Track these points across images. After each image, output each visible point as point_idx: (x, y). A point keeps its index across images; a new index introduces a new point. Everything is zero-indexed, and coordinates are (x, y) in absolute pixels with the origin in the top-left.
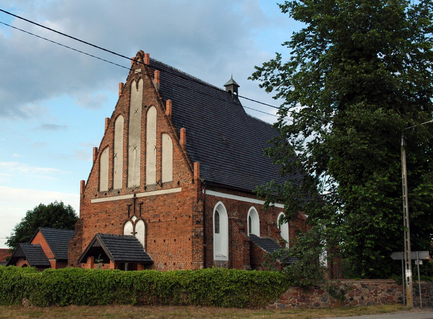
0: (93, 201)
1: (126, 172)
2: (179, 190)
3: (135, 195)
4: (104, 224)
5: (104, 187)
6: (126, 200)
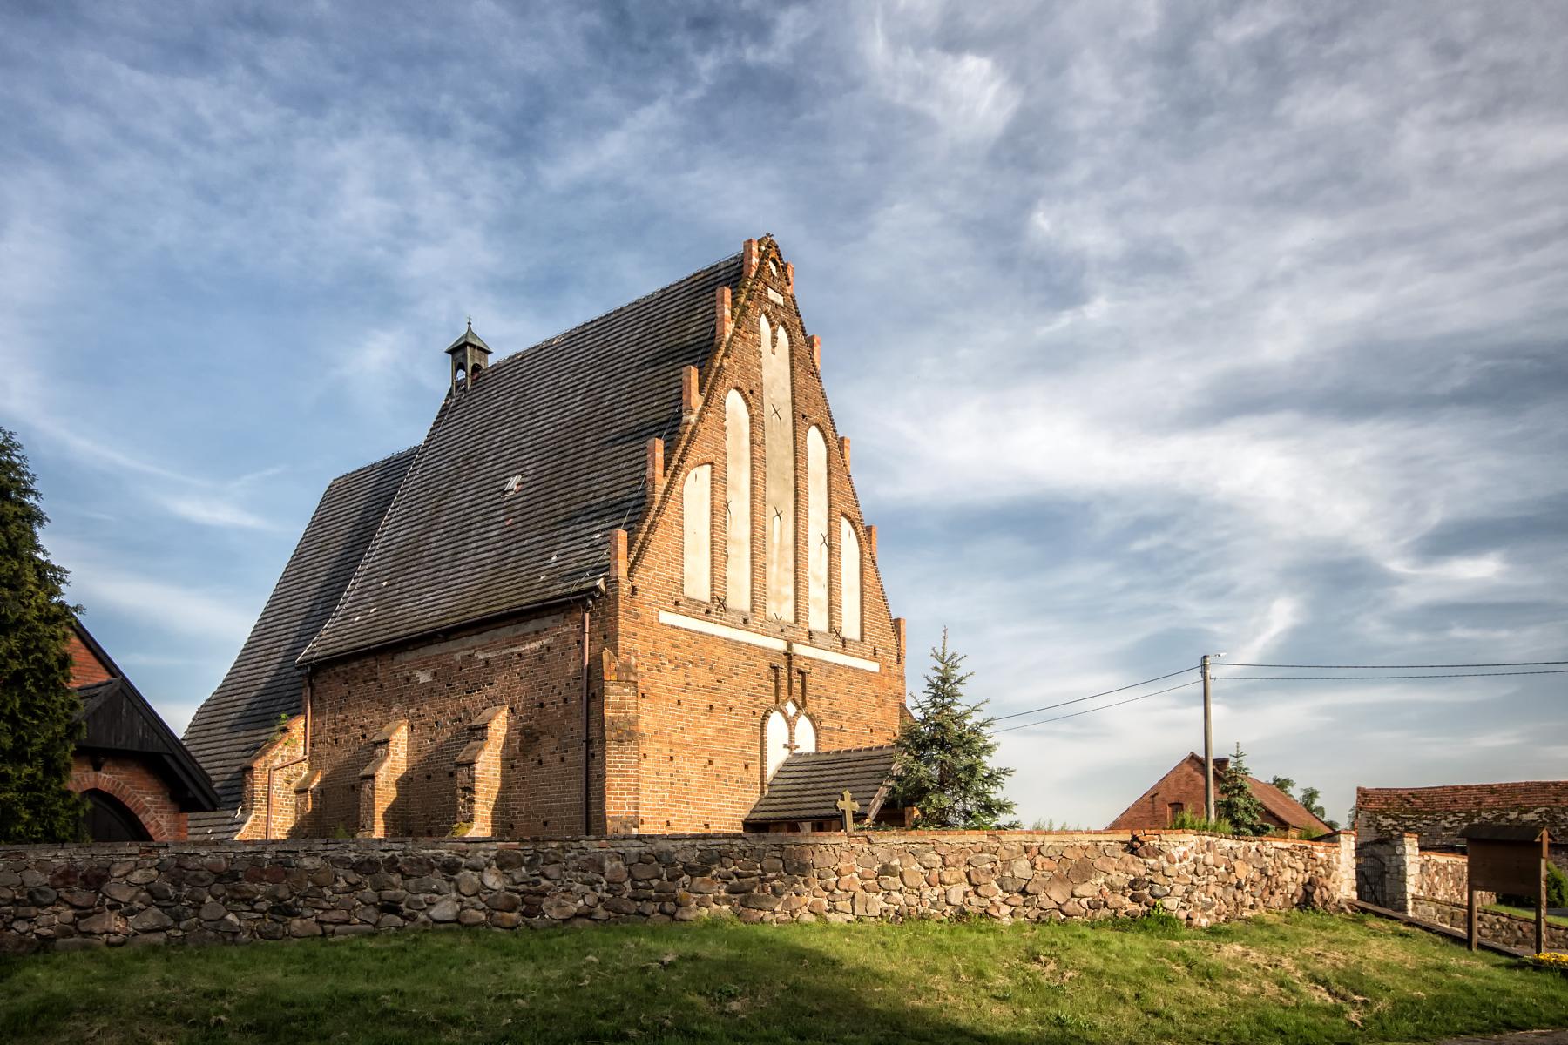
0: (666, 618)
1: (757, 569)
2: (874, 667)
3: (789, 646)
4: (707, 701)
5: (698, 586)
6: (765, 652)
